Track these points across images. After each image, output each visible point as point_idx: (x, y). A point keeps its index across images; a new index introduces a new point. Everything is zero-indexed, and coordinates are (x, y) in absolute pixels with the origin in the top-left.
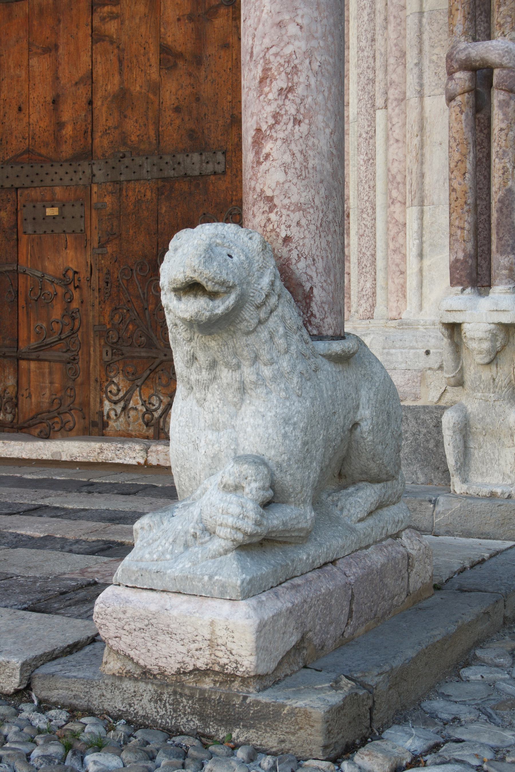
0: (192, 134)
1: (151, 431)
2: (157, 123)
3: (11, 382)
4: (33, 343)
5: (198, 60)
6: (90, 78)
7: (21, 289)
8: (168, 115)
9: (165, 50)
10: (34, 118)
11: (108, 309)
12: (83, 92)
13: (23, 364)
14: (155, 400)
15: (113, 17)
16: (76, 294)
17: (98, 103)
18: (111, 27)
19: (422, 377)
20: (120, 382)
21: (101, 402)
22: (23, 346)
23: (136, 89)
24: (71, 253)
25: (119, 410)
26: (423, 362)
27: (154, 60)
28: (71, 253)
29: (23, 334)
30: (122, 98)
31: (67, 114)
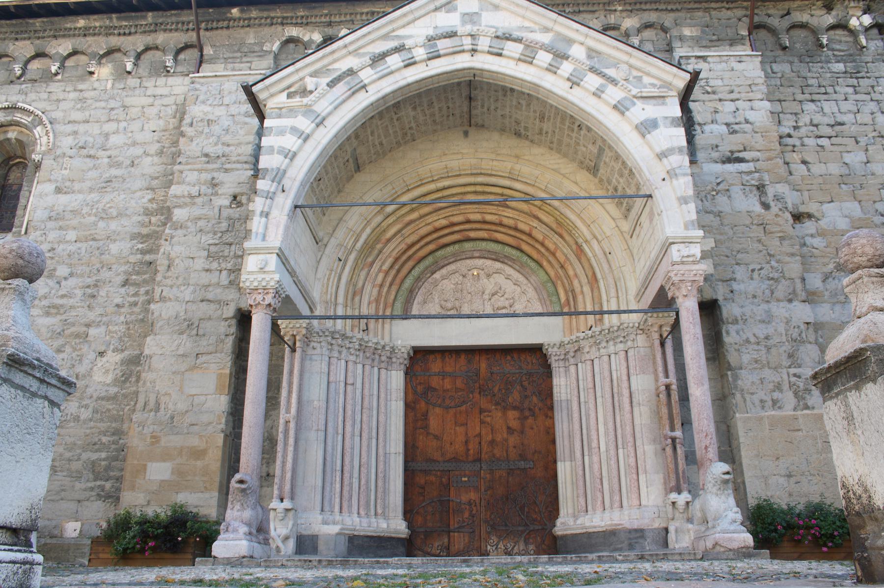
0: (520, 455)
2: (507, 451)
3: (446, 540)
4: (456, 526)
5: (522, 432)
6: (479, 435)
8: (511, 449)
9: (509, 428)
10: (457, 446)
11: (489, 513)
12: (477, 440)
13: (452, 534)
15: (488, 416)
16: (474, 508)
17: (483, 443)
18: (488, 419)
19: (653, 520)
20: (494, 539)
22: (452, 527)
24: (472, 494)
26: (653, 516)
27: (505, 431)
28: (472, 494)
29: (452, 523)
30: (492, 442)
31: (471, 446)
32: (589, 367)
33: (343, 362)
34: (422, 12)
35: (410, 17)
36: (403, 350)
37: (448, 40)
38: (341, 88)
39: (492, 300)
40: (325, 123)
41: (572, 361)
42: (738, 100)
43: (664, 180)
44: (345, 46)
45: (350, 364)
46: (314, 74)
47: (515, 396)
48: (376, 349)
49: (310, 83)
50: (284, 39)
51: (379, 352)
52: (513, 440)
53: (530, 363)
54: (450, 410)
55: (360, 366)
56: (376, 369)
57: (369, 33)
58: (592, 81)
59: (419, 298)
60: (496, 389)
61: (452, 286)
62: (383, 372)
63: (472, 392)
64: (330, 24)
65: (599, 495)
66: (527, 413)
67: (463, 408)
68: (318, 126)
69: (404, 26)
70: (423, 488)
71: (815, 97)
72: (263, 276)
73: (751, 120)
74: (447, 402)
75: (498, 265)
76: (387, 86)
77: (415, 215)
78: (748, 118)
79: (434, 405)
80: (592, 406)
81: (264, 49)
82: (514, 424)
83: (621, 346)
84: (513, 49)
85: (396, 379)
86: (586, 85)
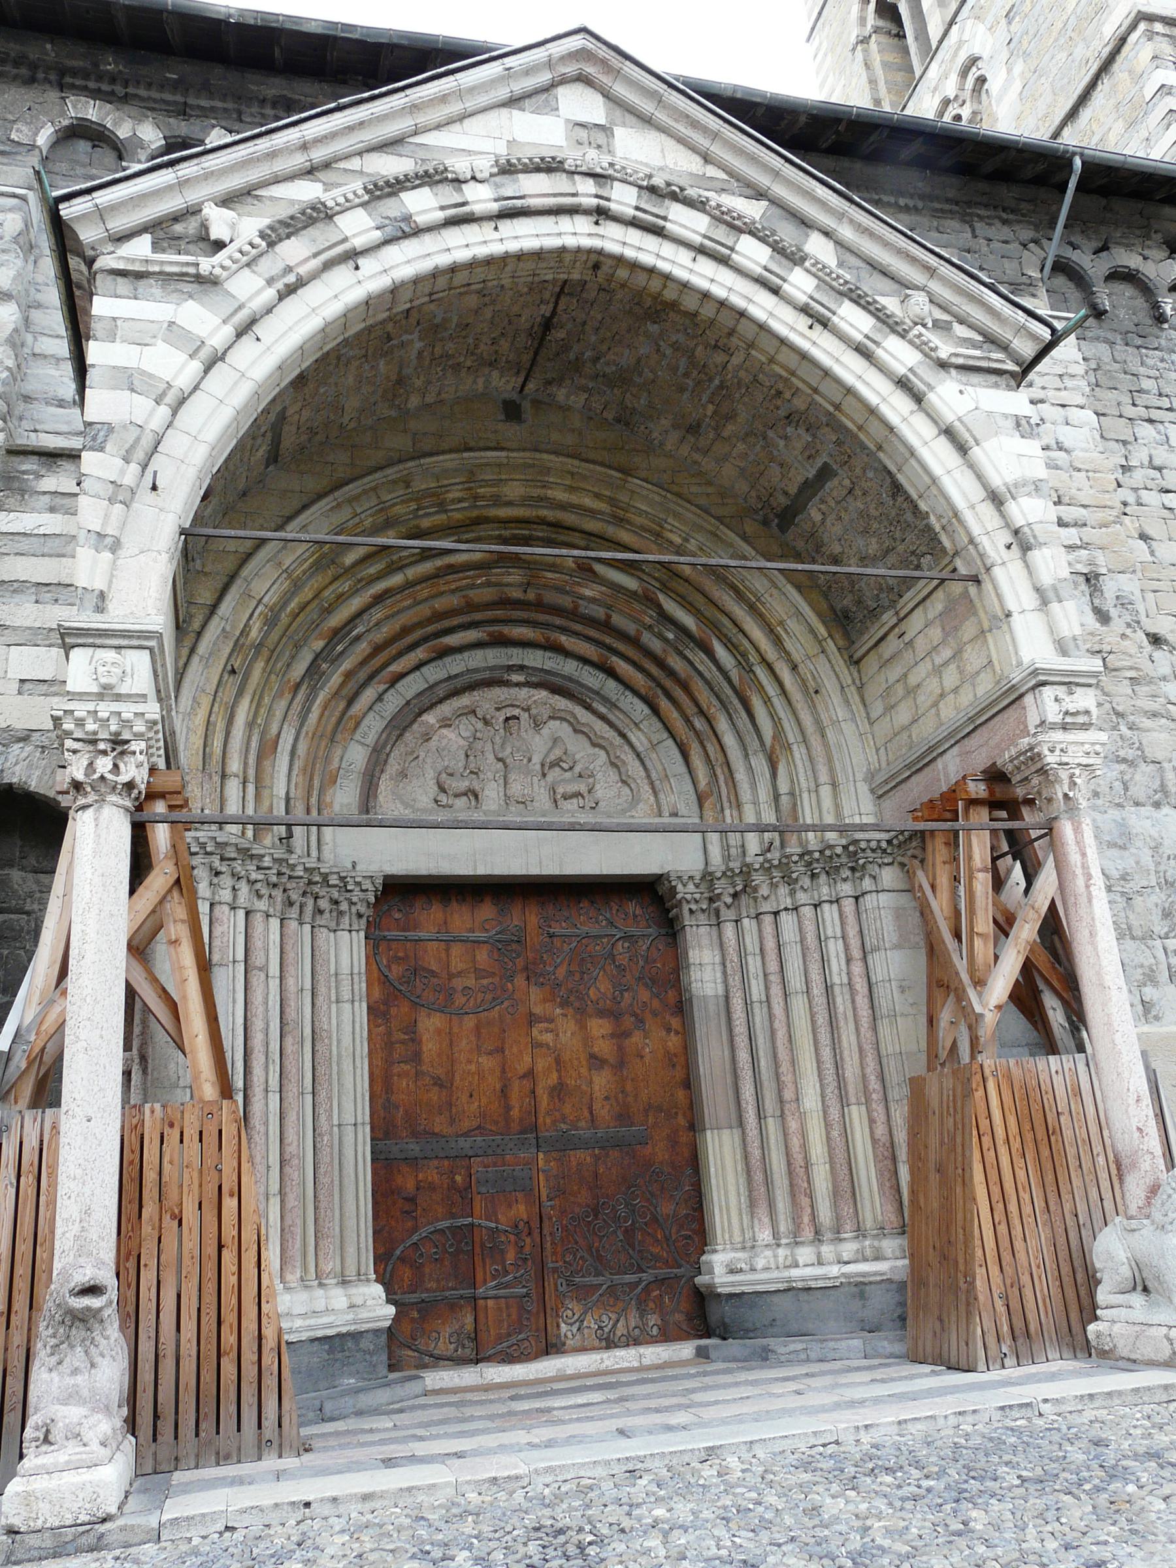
1: (604, 1344)
3: (469, 1319)
5: (621, 1064)
6: (530, 1074)
7: (477, 1239)
9: (593, 1056)
14: (604, 1318)
15: (547, 1031)
17: (539, 1091)
18: (548, 1038)
21: (558, 1326)
23: (571, 1082)
25: (575, 1329)
30: (559, 1091)
32: (768, 929)
33: (241, 914)
34: (483, 100)
35: (455, 108)
36: (367, 885)
37: (542, 176)
38: (296, 251)
39: (550, 778)
40: (258, 329)
41: (727, 914)
42: (1042, 401)
43: (1009, 547)
44: (304, 147)
45: (258, 919)
46: (226, 201)
47: (601, 987)
48: (310, 883)
49: (219, 222)
50: (66, 123)
51: (316, 889)
52: (602, 1082)
53: (633, 916)
54: (466, 1017)
55: (275, 923)
56: (307, 928)
57: (362, 124)
58: (853, 320)
59: (393, 766)
60: (561, 972)
61: (462, 742)
62: (323, 934)
63: (511, 979)
64: (183, 112)
65: (805, 1201)
66: (628, 1021)
67: (495, 1013)
68: (239, 335)
69: (438, 127)
70: (411, 1200)
71: (1155, 414)
72: (116, 707)
73: (1067, 445)
74: (460, 1000)
75: (562, 703)
76: (407, 261)
77: (397, 579)
78: (1061, 439)
79: (432, 1009)
80: (778, 1010)
81: (13, 136)
82: (604, 1048)
83: (846, 889)
84: (685, 221)
85: (348, 951)
86: (843, 326)
